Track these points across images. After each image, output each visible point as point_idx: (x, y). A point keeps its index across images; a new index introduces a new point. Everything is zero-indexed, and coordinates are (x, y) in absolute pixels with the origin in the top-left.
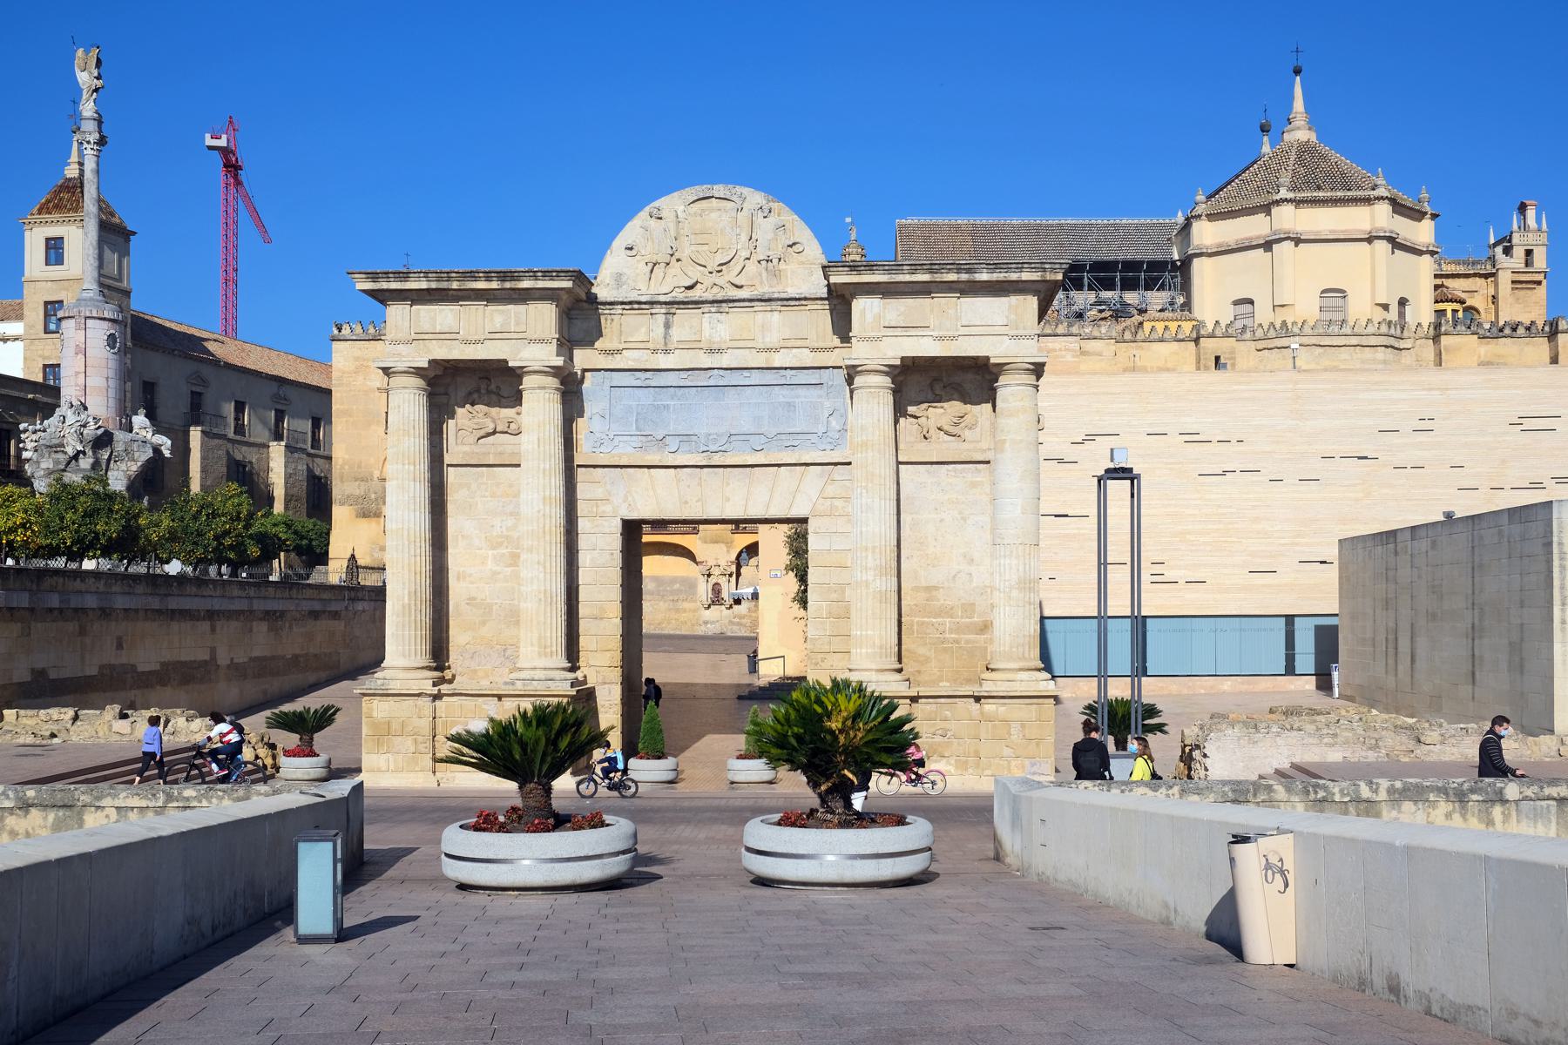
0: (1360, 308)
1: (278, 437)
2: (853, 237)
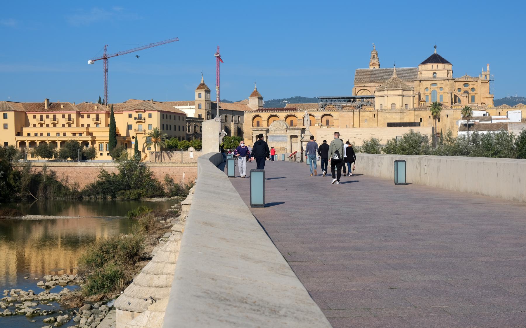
1: (232, 121)
2: (374, 48)
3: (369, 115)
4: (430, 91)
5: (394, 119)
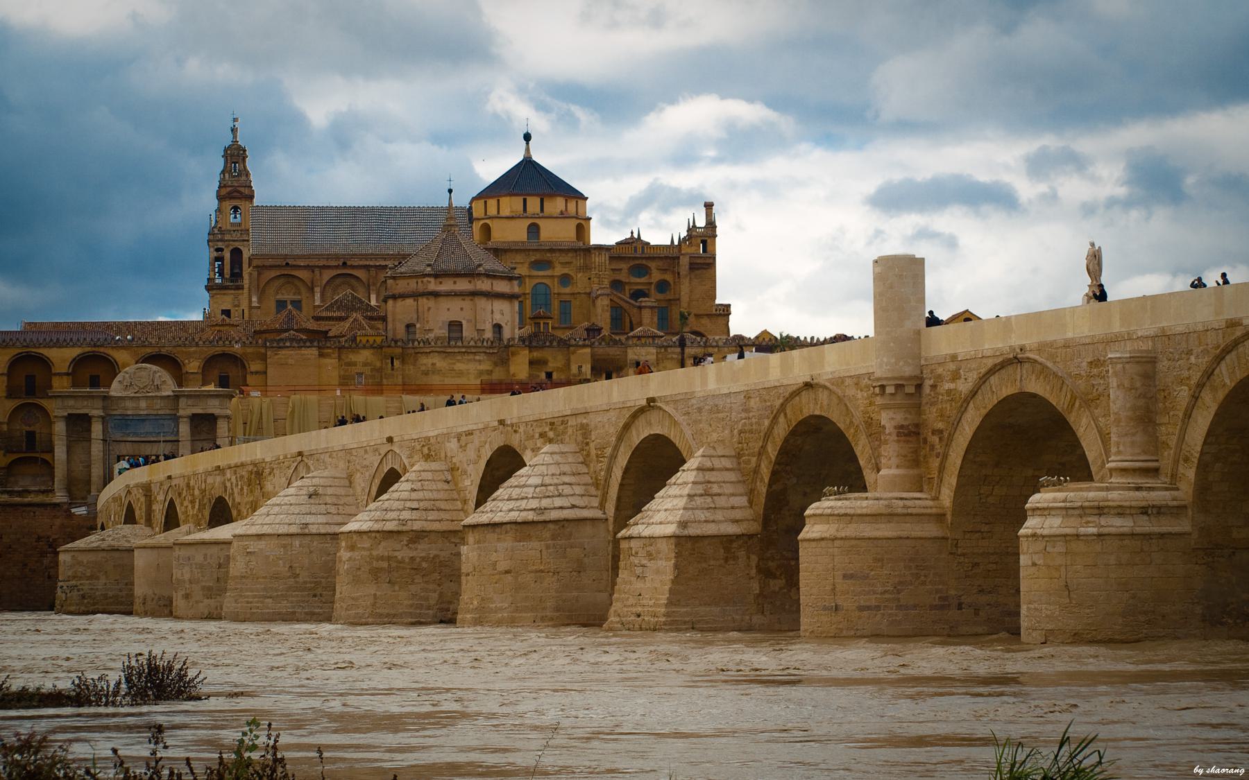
0: (467, 332)
3: (369, 361)
4: (528, 286)
5: (460, 374)
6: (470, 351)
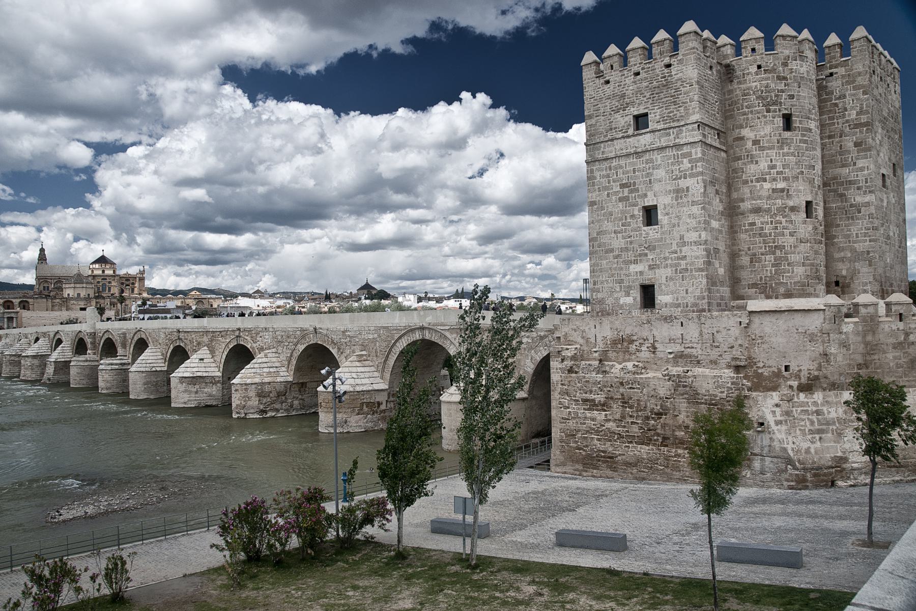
0: (82, 296)
6: (81, 300)
